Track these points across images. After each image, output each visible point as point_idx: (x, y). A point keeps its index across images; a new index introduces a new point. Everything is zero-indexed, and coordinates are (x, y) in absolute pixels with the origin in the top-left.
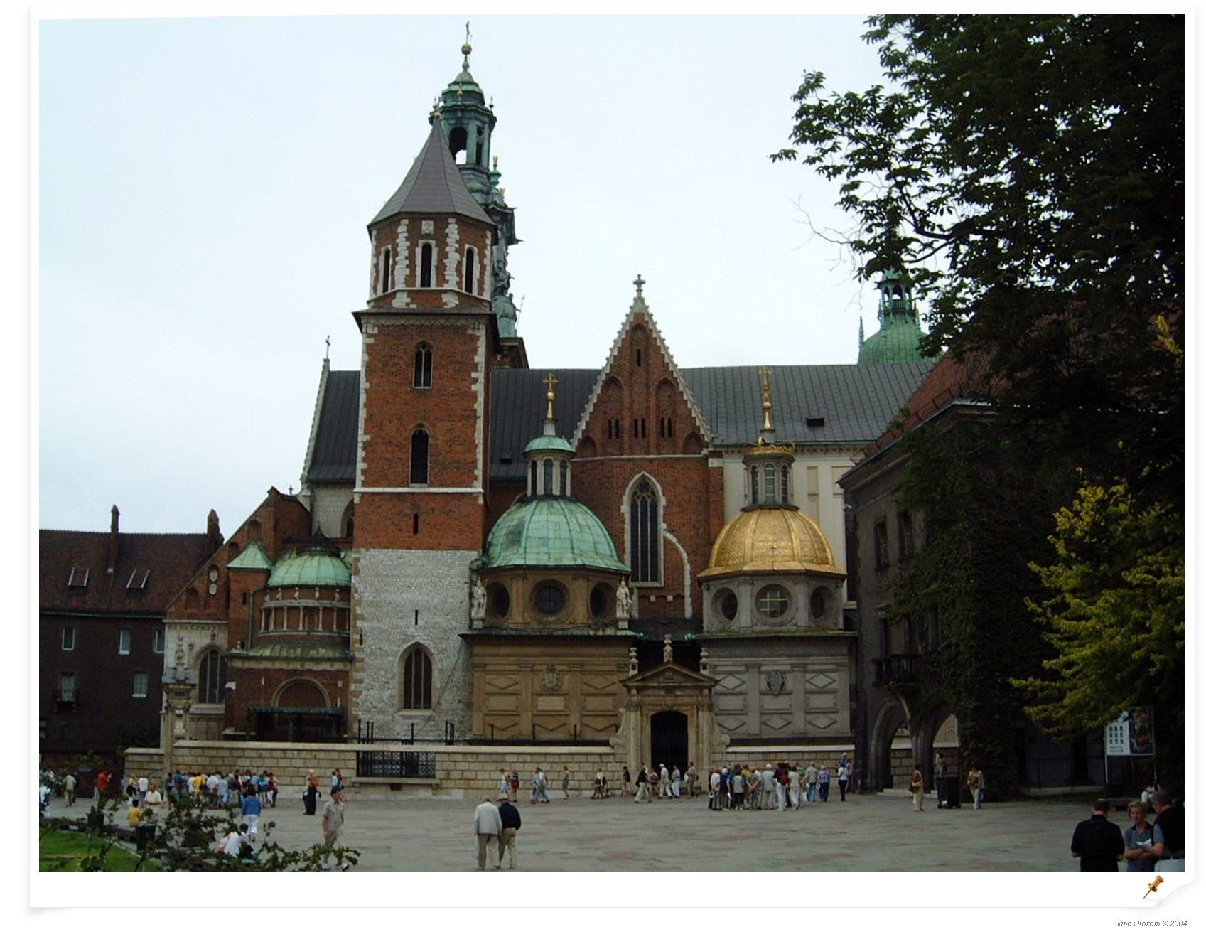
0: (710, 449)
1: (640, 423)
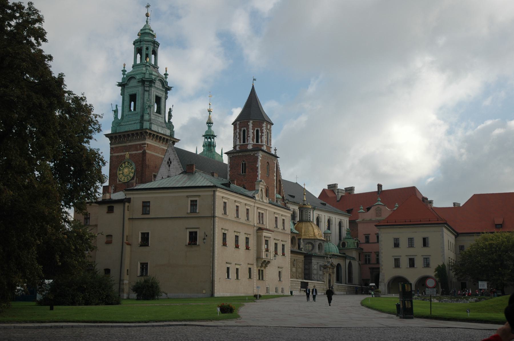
0: (287, 201)
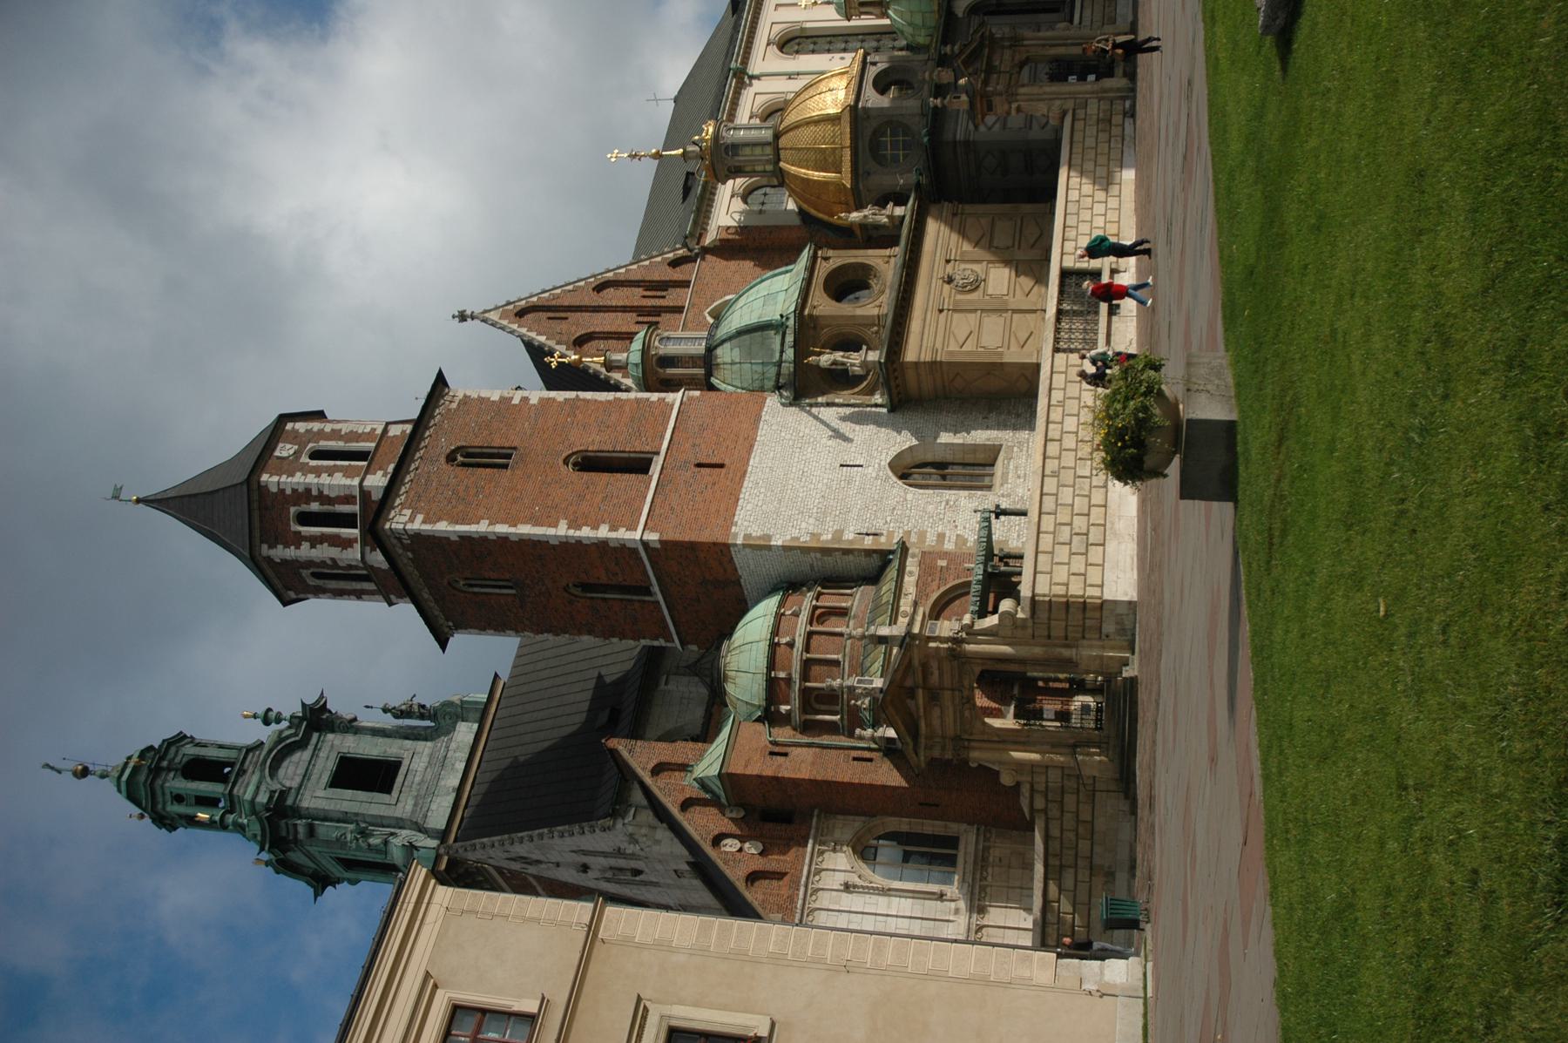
1: (640, 319)
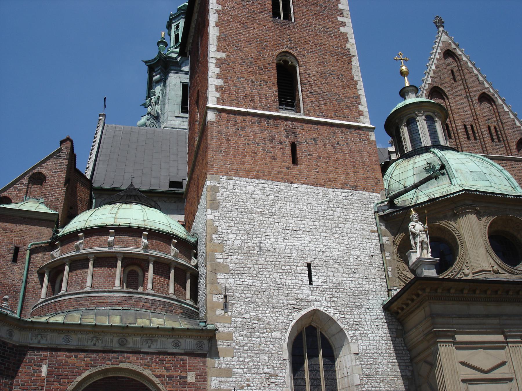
1: (469, 127)
